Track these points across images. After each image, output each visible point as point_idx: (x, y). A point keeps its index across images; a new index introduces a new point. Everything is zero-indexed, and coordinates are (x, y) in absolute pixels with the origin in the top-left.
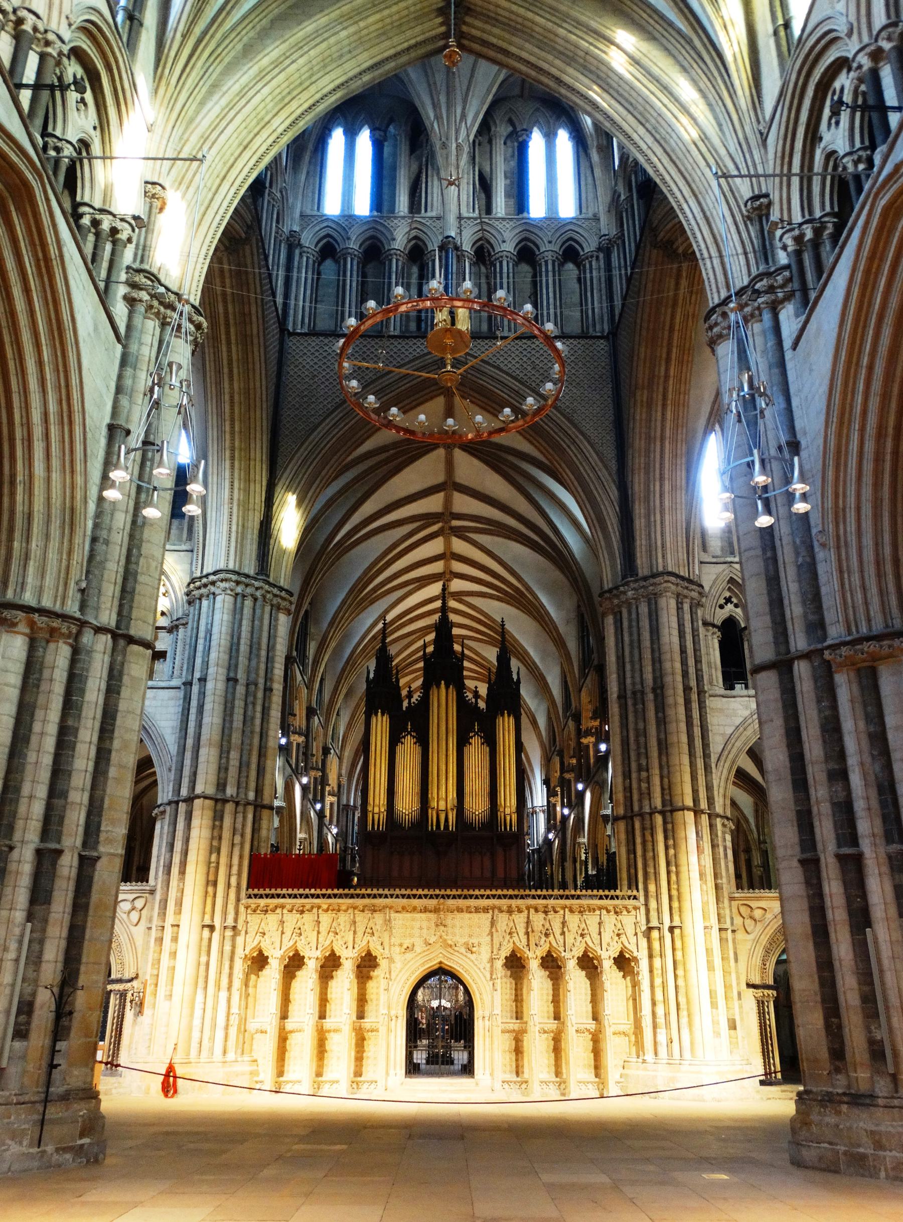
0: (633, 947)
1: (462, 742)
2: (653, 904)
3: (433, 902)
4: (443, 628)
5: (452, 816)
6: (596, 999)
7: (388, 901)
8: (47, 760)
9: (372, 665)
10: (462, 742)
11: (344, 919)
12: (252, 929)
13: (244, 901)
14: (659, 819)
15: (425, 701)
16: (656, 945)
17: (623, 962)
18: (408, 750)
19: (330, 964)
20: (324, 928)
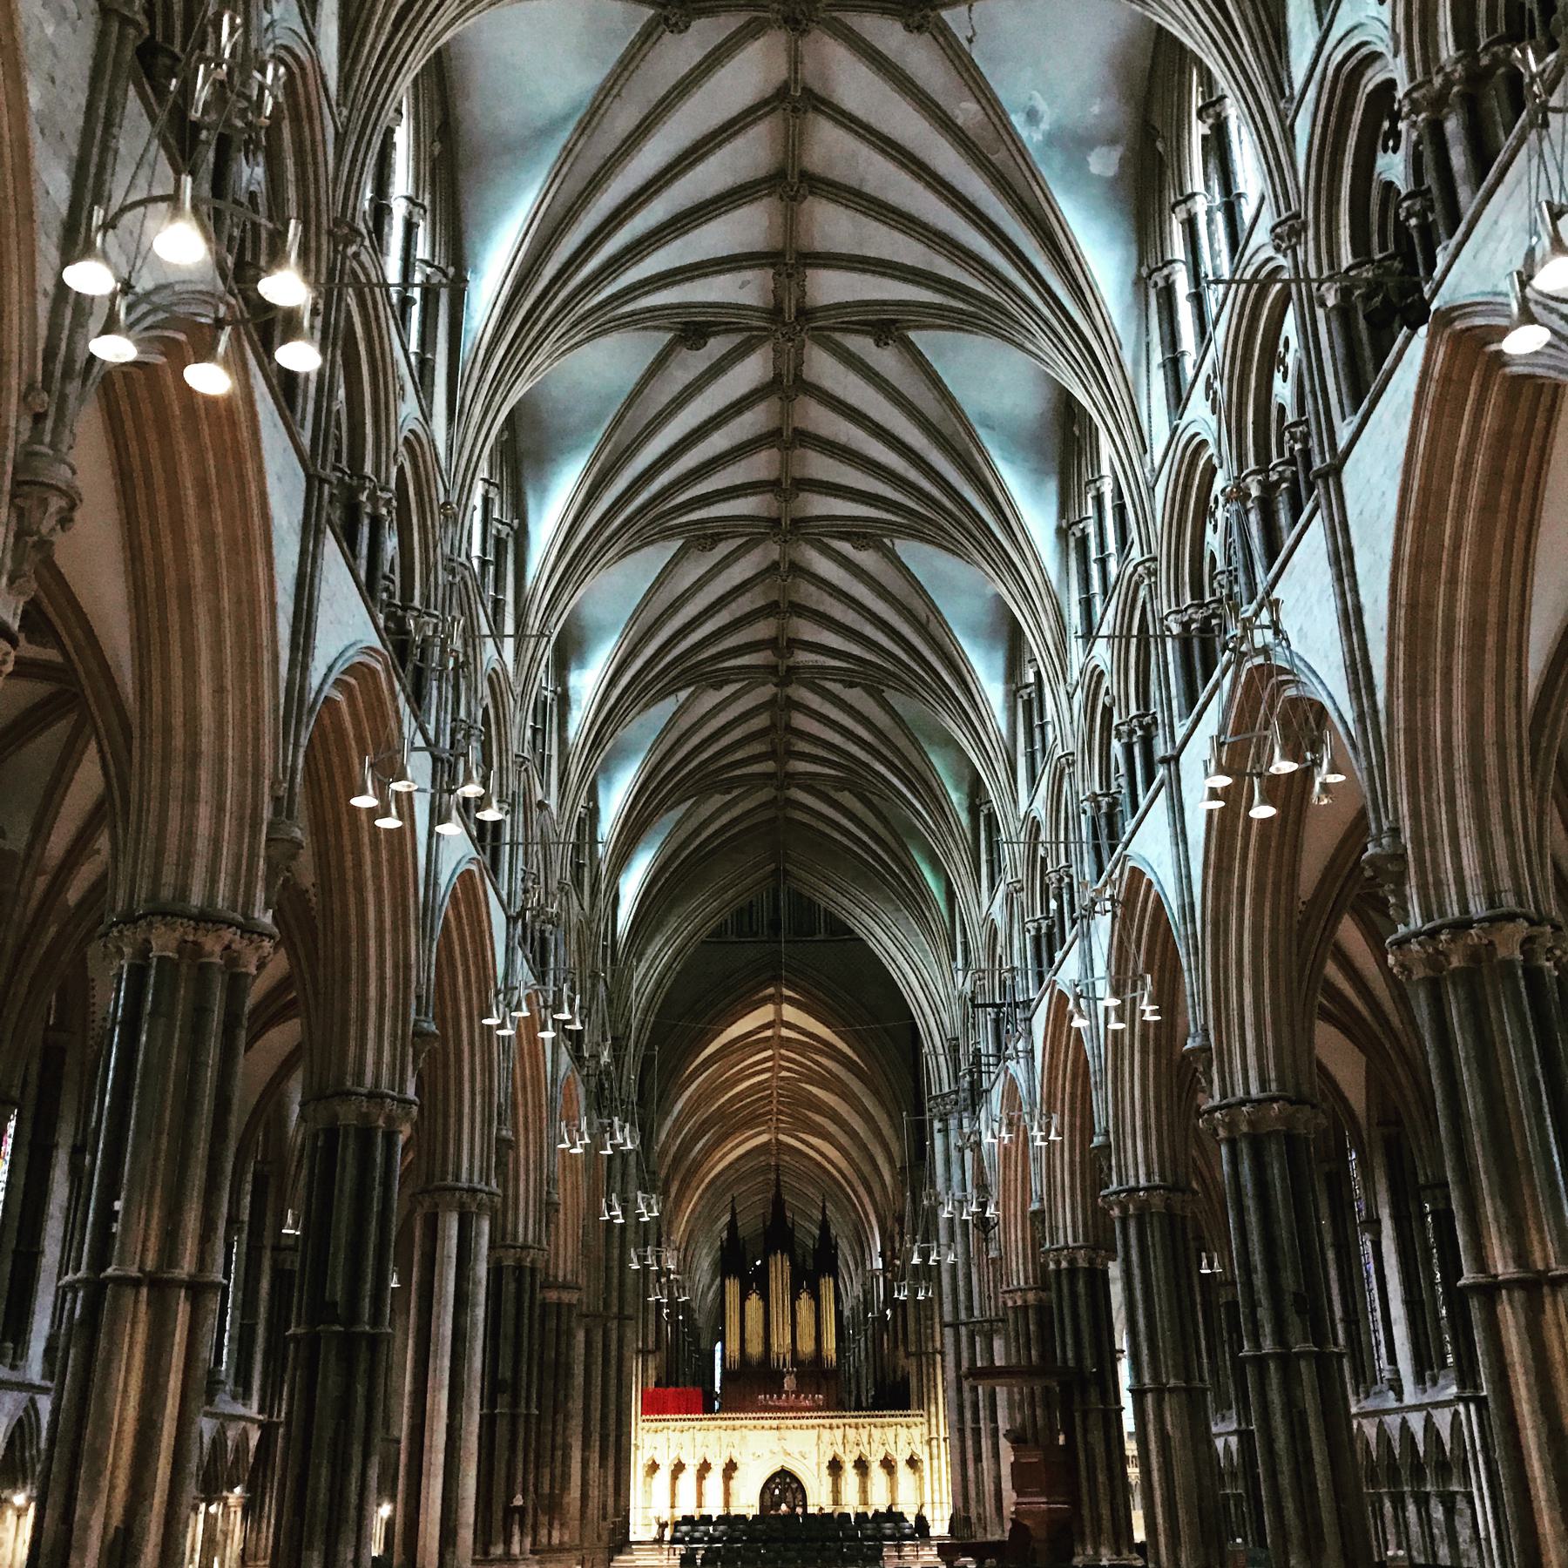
0: (918, 1452)
1: (795, 1297)
2: (933, 1421)
3: (775, 1423)
4: (778, 1195)
5: (788, 1357)
6: (893, 1489)
7: (744, 1422)
8: (599, 1390)
9: (725, 1235)
10: (795, 1297)
11: (713, 1435)
12: (647, 1446)
13: (641, 1424)
14: (938, 1357)
15: (765, 1265)
16: (935, 1451)
17: (912, 1463)
18: (754, 1302)
19: (705, 1467)
20: (698, 1443)
